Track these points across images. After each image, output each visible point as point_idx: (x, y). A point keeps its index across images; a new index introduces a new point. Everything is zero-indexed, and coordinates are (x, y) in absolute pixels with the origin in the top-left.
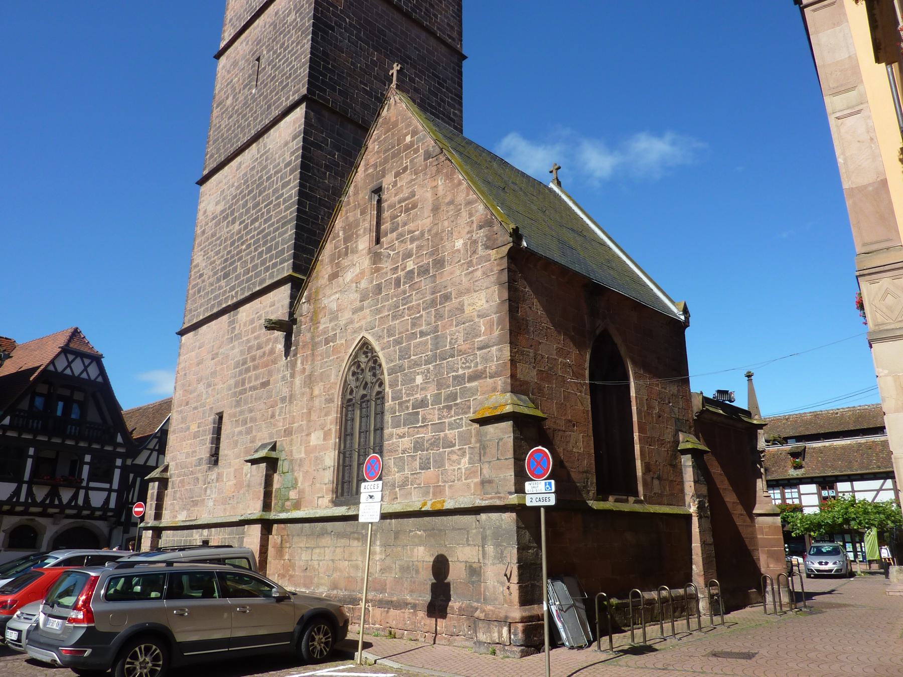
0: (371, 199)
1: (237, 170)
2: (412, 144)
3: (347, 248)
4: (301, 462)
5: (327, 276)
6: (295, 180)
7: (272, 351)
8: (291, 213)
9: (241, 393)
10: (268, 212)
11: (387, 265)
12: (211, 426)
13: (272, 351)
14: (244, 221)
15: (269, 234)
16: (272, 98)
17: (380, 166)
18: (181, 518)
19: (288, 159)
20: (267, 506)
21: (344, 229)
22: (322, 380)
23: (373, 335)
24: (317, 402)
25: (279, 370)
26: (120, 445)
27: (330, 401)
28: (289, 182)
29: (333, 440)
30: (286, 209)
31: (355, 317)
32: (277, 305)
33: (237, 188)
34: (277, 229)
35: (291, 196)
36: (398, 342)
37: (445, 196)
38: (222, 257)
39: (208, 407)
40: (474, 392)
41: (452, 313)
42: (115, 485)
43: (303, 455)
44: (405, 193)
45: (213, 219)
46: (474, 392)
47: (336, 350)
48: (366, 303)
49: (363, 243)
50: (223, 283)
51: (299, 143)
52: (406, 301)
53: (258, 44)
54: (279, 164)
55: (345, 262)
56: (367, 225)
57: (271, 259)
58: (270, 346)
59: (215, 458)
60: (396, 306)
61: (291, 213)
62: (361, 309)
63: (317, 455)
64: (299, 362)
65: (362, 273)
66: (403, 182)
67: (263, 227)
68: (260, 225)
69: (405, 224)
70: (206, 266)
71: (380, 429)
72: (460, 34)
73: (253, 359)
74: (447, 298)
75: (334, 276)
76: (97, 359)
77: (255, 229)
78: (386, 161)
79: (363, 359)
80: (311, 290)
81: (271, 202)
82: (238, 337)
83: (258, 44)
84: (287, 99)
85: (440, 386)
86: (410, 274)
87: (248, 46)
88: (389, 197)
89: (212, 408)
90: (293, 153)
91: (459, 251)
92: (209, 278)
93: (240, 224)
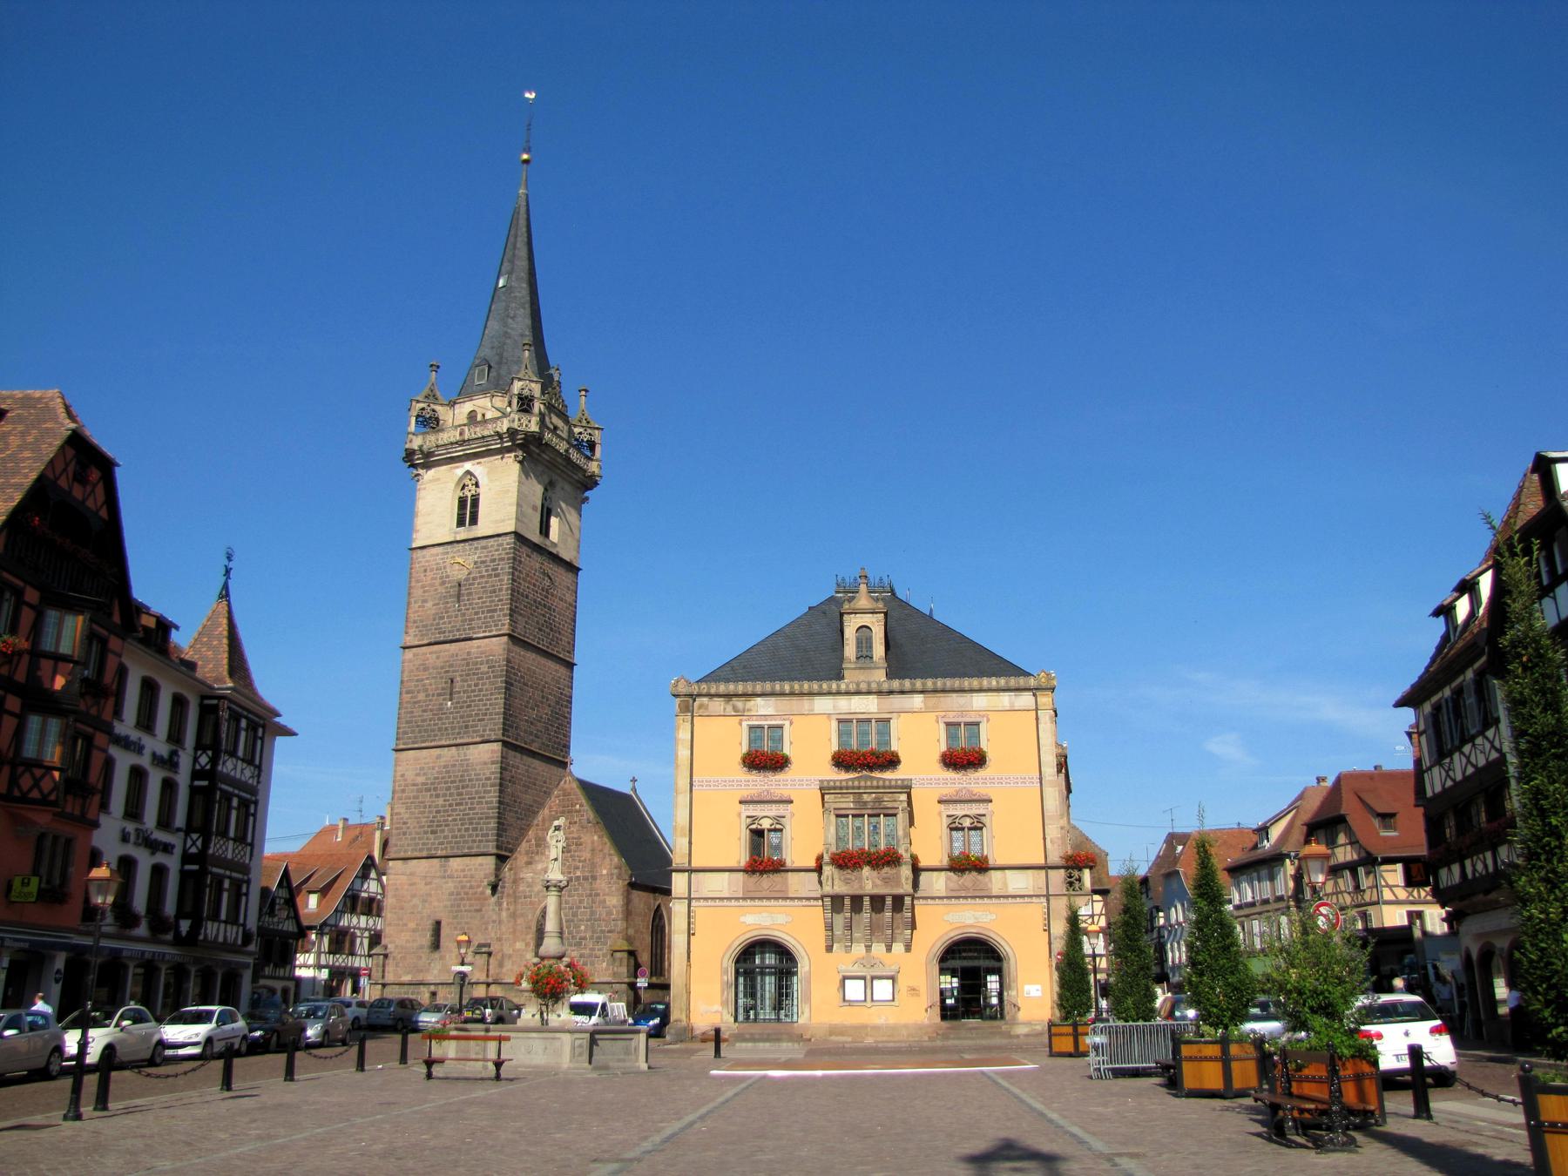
2: (579, 811)
4: (510, 956)
6: (495, 792)
8: (493, 813)
12: (431, 927)
18: (407, 978)
20: (488, 976)
24: (519, 928)
28: (490, 792)
34: (481, 819)
35: (491, 802)
36: (571, 908)
40: (610, 937)
41: (600, 902)
44: (575, 835)
45: (414, 785)
47: (531, 903)
50: (431, 836)
51: (496, 768)
53: (451, 666)
55: (537, 858)
57: (477, 836)
59: (436, 945)
68: (465, 810)
72: (574, 646)
73: (467, 894)
74: (597, 895)
75: (529, 863)
81: (474, 798)
82: (451, 877)
85: (593, 932)
90: (493, 773)
92: (414, 828)
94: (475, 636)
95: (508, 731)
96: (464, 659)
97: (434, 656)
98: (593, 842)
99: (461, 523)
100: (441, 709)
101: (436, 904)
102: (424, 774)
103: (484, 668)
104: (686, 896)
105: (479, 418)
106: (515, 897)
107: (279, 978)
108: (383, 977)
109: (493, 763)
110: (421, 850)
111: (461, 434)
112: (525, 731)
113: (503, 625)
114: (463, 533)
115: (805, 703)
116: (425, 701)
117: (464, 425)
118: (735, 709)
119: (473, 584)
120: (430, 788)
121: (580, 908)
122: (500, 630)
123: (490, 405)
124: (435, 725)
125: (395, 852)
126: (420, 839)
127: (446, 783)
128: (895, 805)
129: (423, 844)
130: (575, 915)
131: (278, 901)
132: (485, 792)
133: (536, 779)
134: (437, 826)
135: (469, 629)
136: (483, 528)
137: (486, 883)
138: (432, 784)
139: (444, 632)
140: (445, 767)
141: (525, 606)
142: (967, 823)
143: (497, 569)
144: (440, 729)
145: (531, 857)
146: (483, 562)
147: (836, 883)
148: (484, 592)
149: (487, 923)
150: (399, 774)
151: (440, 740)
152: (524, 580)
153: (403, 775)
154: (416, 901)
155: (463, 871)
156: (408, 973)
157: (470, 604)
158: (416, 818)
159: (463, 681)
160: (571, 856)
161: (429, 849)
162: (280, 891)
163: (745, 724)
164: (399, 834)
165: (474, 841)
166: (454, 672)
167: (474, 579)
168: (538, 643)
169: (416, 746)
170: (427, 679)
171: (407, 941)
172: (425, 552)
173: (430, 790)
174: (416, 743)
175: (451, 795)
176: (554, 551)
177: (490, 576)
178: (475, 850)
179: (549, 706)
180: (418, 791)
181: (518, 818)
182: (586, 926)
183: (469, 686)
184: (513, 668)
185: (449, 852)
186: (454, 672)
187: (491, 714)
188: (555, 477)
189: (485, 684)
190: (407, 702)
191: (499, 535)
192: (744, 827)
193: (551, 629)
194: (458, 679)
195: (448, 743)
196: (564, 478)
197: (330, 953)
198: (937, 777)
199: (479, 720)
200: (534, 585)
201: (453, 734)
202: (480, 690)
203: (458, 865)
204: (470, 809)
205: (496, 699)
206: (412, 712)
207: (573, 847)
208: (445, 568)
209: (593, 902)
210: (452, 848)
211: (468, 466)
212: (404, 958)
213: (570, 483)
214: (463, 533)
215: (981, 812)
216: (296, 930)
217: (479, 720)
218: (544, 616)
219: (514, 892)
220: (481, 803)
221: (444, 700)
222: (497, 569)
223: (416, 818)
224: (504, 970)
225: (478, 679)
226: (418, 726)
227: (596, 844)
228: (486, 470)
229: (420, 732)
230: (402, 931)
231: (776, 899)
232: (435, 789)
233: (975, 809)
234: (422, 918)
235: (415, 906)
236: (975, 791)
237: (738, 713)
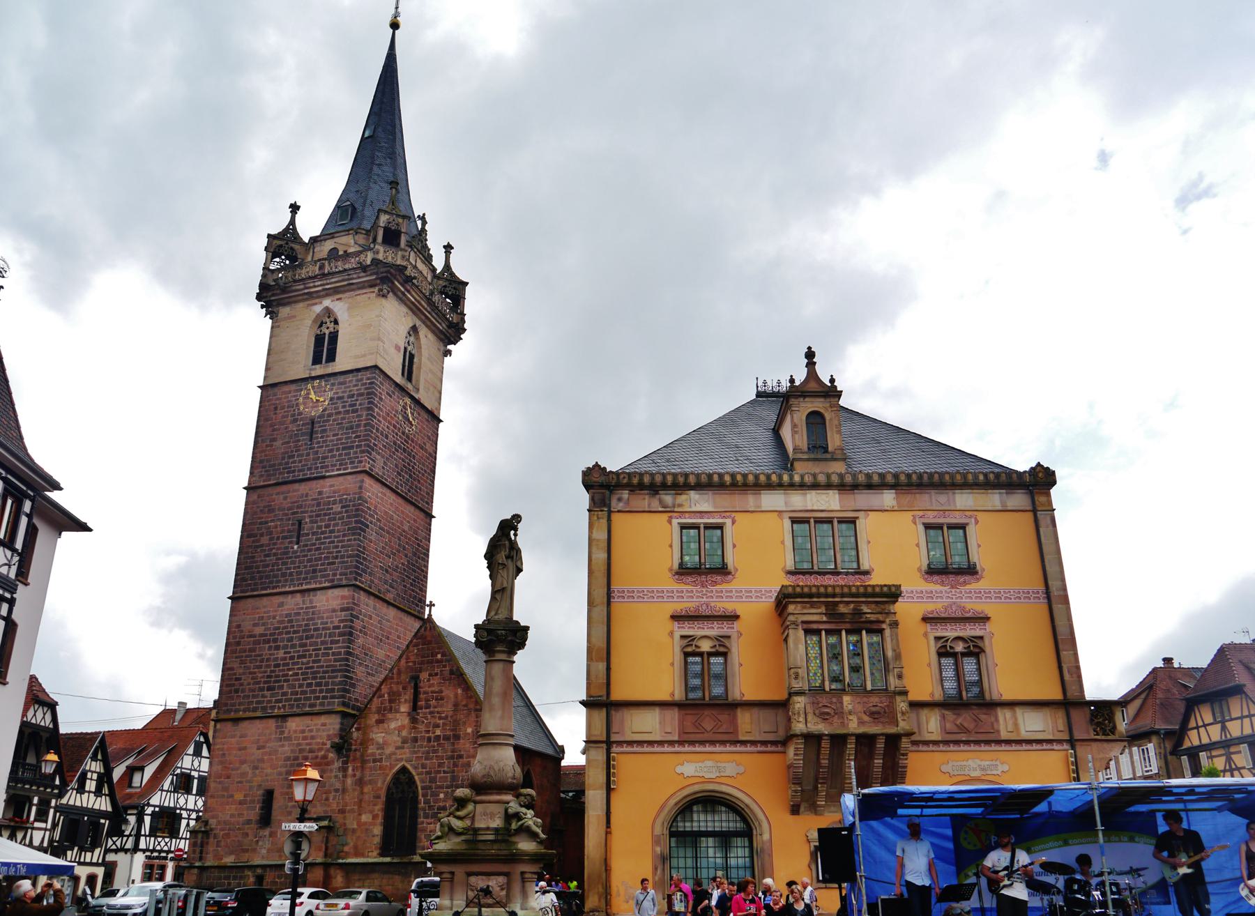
0: (409, 682)
1: (278, 607)
3: (391, 708)
4: (354, 831)
5: (374, 720)
7: (325, 757)
10: (317, 655)
11: (422, 727)
14: (290, 653)
15: (319, 672)
16: (317, 565)
17: (419, 664)
19: (337, 624)
21: (389, 694)
22: (371, 784)
23: (411, 765)
24: (366, 797)
25: (331, 771)
26: (57, 787)
27: (379, 797)
28: (338, 642)
29: (380, 820)
30: (335, 660)
31: (397, 751)
32: (328, 727)
33: (281, 622)
34: (327, 672)
35: (340, 653)
36: (427, 773)
37: (462, 701)
38: (265, 672)
39: (255, 784)
41: (463, 766)
42: (49, 827)
43: (355, 826)
44: (436, 689)
45: (251, 636)
48: (406, 745)
49: (404, 708)
52: (435, 751)
53: (298, 507)
54: (327, 623)
55: (390, 716)
56: (407, 697)
57: (321, 691)
58: (323, 753)
60: (428, 752)
61: (340, 665)
62: (403, 748)
63: (367, 827)
64: (350, 769)
65: (403, 727)
66: (435, 681)
67: (311, 665)
68: (308, 663)
69: (435, 707)
70: (244, 674)
71: (414, 817)
74: (461, 757)
75: (379, 722)
76: (52, 706)
77: (303, 664)
78: (422, 663)
79: (402, 777)
80: (359, 724)
81: (320, 649)
82: (288, 739)
83: (298, 507)
84: (335, 575)
86: (439, 737)
87: (285, 502)
88: (424, 687)
91: (469, 734)
92: (249, 684)
93: (285, 653)
94: (328, 474)
95: (361, 575)
96: (313, 500)
97: (281, 497)
99: (317, 360)
100: (287, 553)
101: (269, 771)
102: (263, 624)
103: (337, 508)
104: (604, 738)
105: (341, 253)
107: (85, 864)
108: (201, 859)
109: (343, 610)
110: (255, 710)
111: (321, 268)
112: (380, 579)
113: (361, 462)
114: (319, 370)
115: (750, 500)
116: (269, 545)
117: (323, 259)
118: (661, 501)
119: (329, 421)
121: (439, 772)
122: (357, 467)
123: (352, 241)
124: (278, 570)
126: (254, 696)
127: (288, 633)
128: (880, 617)
129: (258, 702)
130: (433, 780)
131: (89, 775)
132: (332, 642)
133: (390, 633)
134: (275, 682)
135: (322, 467)
136: (343, 362)
137: (329, 746)
138: (271, 635)
139: (294, 471)
140: (287, 615)
141: (385, 446)
142: (960, 647)
143: (355, 405)
145: (384, 715)
146: (339, 398)
147: (810, 717)
148: (339, 429)
149: (328, 792)
150: (234, 624)
151: (285, 586)
152: (385, 419)
153: (239, 626)
155: (303, 731)
156: (231, 853)
157: (324, 442)
158: (250, 673)
159: (312, 522)
160: (431, 713)
161: (264, 709)
162: (94, 763)
163: (675, 521)
164: (230, 692)
165: (318, 698)
166: (302, 512)
167: (330, 415)
168: (396, 487)
169: (255, 593)
170: (272, 521)
171: (232, 816)
172: (276, 390)
173: (269, 641)
174: (257, 590)
175: (293, 646)
176: (416, 396)
177: (347, 412)
179: (406, 556)
180: (255, 643)
181: (369, 674)
182: (446, 794)
183: (320, 527)
184: (369, 509)
185: (288, 711)
186: (302, 512)
187: (343, 557)
188: (418, 323)
189: (337, 525)
190: (249, 546)
191: (358, 370)
192: (677, 650)
193: (411, 476)
194: (307, 520)
195: (292, 589)
196: (427, 326)
197: (150, 836)
198: (919, 589)
199: (329, 564)
200: (395, 426)
201: (298, 579)
202: (331, 532)
203: (297, 726)
204: (314, 662)
205: (348, 541)
206: (254, 557)
207: (433, 702)
208: (297, 405)
210: (292, 706)
211: (327, 302)
212: (228, 835)
213: (433, 332)
214: (319, 370)
215: (978, 633)
216: (110, 809)
217: (329, 564)
218: (403, 460)
219: (362, 756)
220: (328, 654)
221: (290, 542)
222: (355, 405)
223: (250, 673)
225: (330, 520)
226: (259, 572)
227: (460, 698)
228: (347, 305)
230: (228, 804)
231: (723, 743)
233: (970, 631)
234: (251, 788)
235: (244, 774)
236: (968, 606)
237: (668, 511)
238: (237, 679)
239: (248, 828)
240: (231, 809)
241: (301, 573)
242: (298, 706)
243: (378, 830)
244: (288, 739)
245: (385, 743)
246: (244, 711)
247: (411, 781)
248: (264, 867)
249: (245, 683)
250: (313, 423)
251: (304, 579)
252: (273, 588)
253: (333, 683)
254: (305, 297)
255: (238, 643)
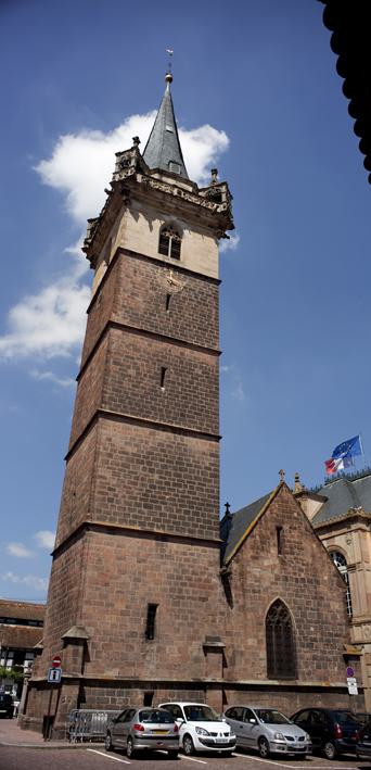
4: (242, 653)
7: (207, 581)
9: (178, 597)
11: (290, 569)
13: (207, 581)
18: (112, 674)
40: (338, 641)
44: (297, 540)
45: (123, 453)
46: (338, 641)
49: (274, 551)
50: (146, 510)
52: (303, 591)
55: (262, 554)
57: (199, 520)
59: (150, 633)
60: (297, 591)
66: (295, 533)
73: (190, 579)
75: (255, 558)
82: (169, 557)
86: (303, 579)
89: (143, 599)
93: (161, 477)
98: (312, 548)
102: (136, 445)
106: (244, 590)
108: (82, 673)
110: (134, 523)
120: (146, 459)
125: (98, 519)
127: (162, 460)
129: (134, 516)
130: (304, 615)
132: (205, 480)
134: (152, 501)
140: (159, 444)
144: (153, 408)
154: (125, 578)
155: (184, 554)
156: (114, 667)
165: (196, 526)
171: (114, 626)
173: (142, 463)
178: (197, 536)
207: (296, 550)
209: (319, 605)
211: (174, 218)
212: (107, 647)
219: (242, 585)
224: (237, 668)
226: (127, 397)
229: (130, 403)
232: (149, 463)
234: (133, 599)
238: (110, 489)
239: (133, 641)
240: (111, 619)
241: (170, 412)
242: (177, 530)
243: (263, 654)
244: (169, 557)
245: (261, 577)
246: (121, 521)
247: (285, 612)
248: (156, 685)
249: (120, 495)
250: (169, 296)
251: (174, 418)
252: (144, 416)
253: (209, 516)
254: (159, 205)
255: (110, 455)
